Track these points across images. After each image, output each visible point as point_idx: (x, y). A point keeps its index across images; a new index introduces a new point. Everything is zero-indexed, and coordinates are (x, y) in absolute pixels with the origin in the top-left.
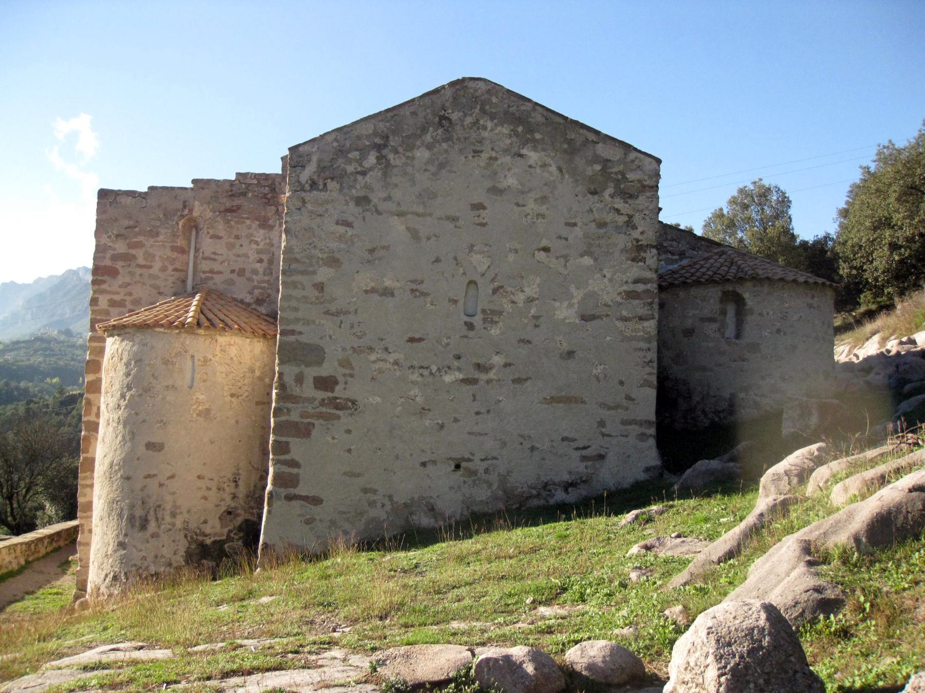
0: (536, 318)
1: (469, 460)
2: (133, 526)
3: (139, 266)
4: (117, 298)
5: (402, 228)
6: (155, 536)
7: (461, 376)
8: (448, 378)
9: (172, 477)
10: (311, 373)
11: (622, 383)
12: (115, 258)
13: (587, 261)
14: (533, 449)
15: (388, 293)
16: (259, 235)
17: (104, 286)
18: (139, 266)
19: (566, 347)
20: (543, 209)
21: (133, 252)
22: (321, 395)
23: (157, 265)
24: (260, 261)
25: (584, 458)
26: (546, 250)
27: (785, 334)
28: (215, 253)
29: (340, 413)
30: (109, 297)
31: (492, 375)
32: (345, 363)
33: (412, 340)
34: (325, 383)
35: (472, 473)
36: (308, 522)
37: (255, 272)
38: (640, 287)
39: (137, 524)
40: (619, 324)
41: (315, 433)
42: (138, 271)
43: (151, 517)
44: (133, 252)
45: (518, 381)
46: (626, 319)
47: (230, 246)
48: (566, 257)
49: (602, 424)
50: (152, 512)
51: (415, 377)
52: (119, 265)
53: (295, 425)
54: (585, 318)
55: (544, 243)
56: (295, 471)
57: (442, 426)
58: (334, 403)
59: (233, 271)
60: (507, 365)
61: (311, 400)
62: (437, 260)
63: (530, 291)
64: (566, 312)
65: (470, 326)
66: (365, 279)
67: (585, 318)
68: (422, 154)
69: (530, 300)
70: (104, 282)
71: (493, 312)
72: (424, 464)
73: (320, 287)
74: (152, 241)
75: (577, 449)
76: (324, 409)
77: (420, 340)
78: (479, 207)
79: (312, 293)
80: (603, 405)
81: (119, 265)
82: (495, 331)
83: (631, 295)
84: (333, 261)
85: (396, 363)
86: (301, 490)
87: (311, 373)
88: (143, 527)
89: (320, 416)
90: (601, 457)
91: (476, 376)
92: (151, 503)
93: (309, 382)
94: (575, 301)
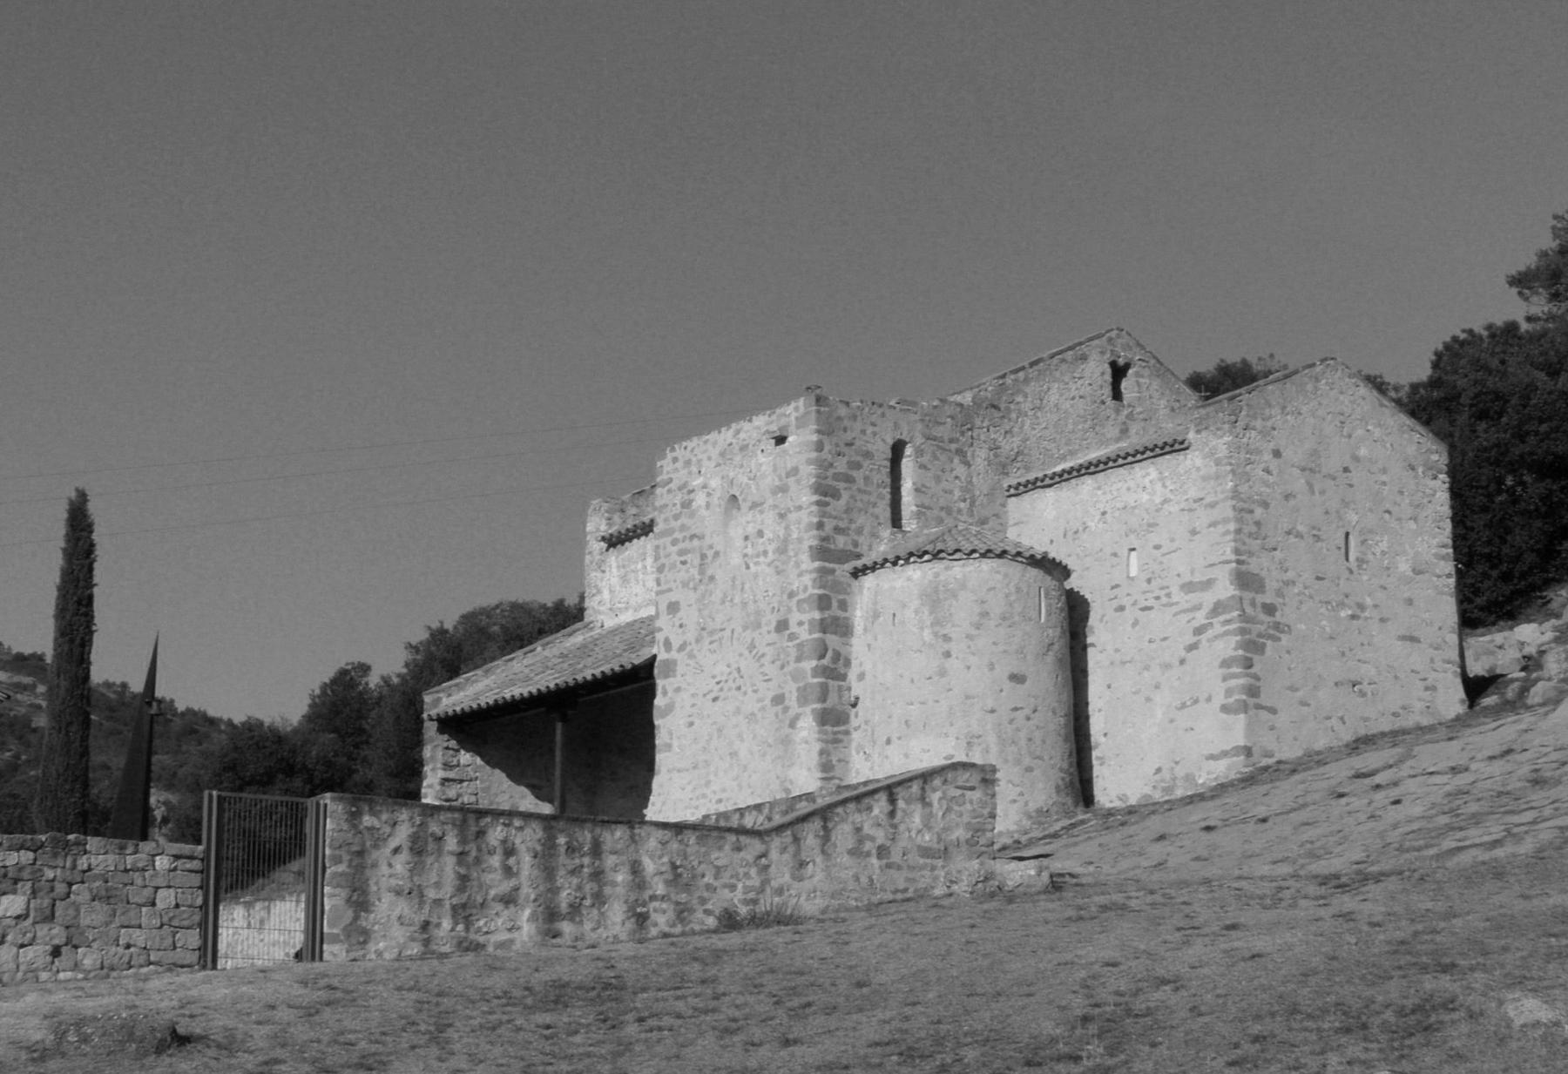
4: (842, 525)
8: (1343, 614)
10: (1260, 599)
12: (836, 477)
14: (1396, 677)
15: (1299, 536)
17: (828, 509)
18: (859, 490)
19: (1406, 595)
20: (1384, 478)
26: (1388, 512)
30: (835, 522)
32: (1279, 593)
33: (1318, 578)
34: (1270, 609)
35: (1362, 694)
37: (960, 511)
38: (1445, 551)
47: (938, 479)
49: (1432, 660)
51: (1323, 610)
52: (841, 485)
53: (1254, 643)
54: (1417, 572)
55: (1388, 506)
58: (1277, 626)
60: (1376, 606)
63: (1384, 546)
64: (1404, 567)
65: (1351, 572)
70: (827, 504)
73: (1258, 524)
78: (1346, 470)
79: (1254, 529)
80: (1431, 646)
82: (1365, 578)
83: (1443, 558)
84: (1265, 505)
87: (1260, 599)
89: (1271, 637)
90: (1433, 688)
93: (1259, 609)
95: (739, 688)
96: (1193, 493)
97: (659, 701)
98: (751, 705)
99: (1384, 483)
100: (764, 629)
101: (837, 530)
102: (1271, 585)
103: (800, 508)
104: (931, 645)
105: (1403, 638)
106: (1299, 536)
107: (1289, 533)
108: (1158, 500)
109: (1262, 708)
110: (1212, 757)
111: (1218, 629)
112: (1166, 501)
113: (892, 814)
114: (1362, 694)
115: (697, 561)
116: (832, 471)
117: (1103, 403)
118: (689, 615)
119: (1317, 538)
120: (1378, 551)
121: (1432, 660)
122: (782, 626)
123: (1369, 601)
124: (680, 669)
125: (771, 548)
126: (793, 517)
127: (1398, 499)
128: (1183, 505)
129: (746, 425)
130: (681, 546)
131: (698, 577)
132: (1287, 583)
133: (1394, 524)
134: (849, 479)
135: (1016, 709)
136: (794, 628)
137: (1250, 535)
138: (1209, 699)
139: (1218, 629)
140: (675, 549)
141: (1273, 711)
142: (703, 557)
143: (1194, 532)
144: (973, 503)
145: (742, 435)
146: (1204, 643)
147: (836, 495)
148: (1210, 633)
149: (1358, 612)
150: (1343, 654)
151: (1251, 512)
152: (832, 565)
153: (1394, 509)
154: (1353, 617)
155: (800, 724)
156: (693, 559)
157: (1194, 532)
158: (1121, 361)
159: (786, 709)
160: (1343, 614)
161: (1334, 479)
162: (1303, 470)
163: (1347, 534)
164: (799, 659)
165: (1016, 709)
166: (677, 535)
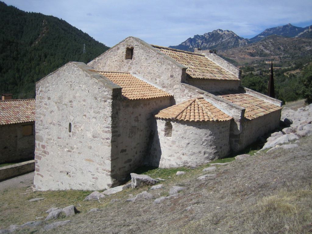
0: (83, 135)
1: (70, 173)
7: (68, 150)
11: (102, 158)
13: (94, 120)
14: (82, 172)
19: (90, 145)
20: (84, 103)
22: (42, 149)
25: (93, 178)
26: (85, 116)
27: (185, 138)
33: (59, 138)
34: (43, 147)
36: (41, 181)
38: (107, 129)
40: (102, 140)
41: (42, 159)
48: (89, 118)
49: (97, 169)
54: (94, 137)
58: (45, 152)
64: (89, 135)
65: (70, 136)
72: (61, 172)
73: (41, 121)
75: (92, 175)
77: (60, 138)
87: (41, 144)
90: (97, 178)
91: (71, 150)
94: (91, 132)
99: (84, 105)
105: (87, 160)
106: (54, 125)
107: (51, 123)
109: (40, 175)
114: (70, 176)
117: (123, 61)
119: (60, 125)
123: (75, 146)
127: (89, 111)
132: (49, 139)
141: (42, 176)
153: (88, 115)
154: (69, 151)
160: (66, 150)
163: (70, 124)
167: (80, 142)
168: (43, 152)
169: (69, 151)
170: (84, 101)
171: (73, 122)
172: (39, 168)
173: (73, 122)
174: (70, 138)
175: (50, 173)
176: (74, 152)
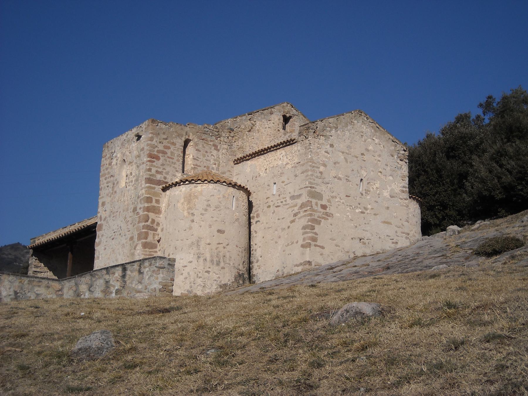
0: (379, 194)
2: (213, 264)
3: (168, 157)
4: (160, 170)
5: (343, 157)
6: (223, 268)
8: (357, 211)
9: (228, 245)
10: (320, 203)
12: (158, 151)
13: (391, 178)
14: (380, 238)
15: (340, 179)
16: (215, 152)
17: (154, 164)
18: (168, 157)
19: (386, 205)
20: (379, 159)
21: (166, 150)
22: (323, 211)
23: (176, 158)
24: (215, 164)
25: (393, 243)
26: (381, 172)
28: (198, 157)
29: (329, 218)
30: (157, 169)
31: (368, 211)
32: (329, 201)
34: (324, 207)
35: (364, 244)
36: (321, 255)
37: (213, 168)
38: (404, 189)
39: (215, 263)
40: (400, 200)
41: (322, 224)
42: (168, 160)
43: (221, 260)
44: (166, 150)
45: (375, 214)
46: (401, 199)
48: (386, 175)
49: (396, 232)
50: (222, 258)
51: (348, 209)
52: (160, 155)
53: (316, 220)
54: (392, 197)
55: (380, 170)
56: (316, 236)
57: (356, 227)
58: (327, 214)
59: (205, 167)
60: (372, 209)
61: (320, 212)
62: (353, 170)
63: (377, 185)
64: (386, 194)
66: (333, 173)
67: (392, 197)
68: (347, 133)
69: (377, 188)
70: (154, 162)
71: (368, 191)
72: (352, 239)
73: (321, 173)
74: (173, 147)
76: (324, 216)
77: (349, 196)
78: (362, 154)
79: (319, 175)
80: (396, 226)
81: (160, 155)
82: (368, 197)
83: (403, 192)
84: (325, 165)
85: (343, 203)
86: (318, 243)
87: (320, 203)
88: (218, 264)
89: (323, 218)
90: (397, 243)
92: (221, 254)
93: (319, 206)
95: (120, 234)
96: (296, 161)
97: (97, 240)
98: (124, 241)
99: (379, 161)
100: (129, 211)
101: (157, 172)
102: (326, 197)
103: (143, 163)
104: (187, 217)
105: (384, 222)
107: (335, 177)
108: (285, 163)
110: (297, 265)
111: (302, 214)
112: (287, 164)
113: (124, 276)
114: (364, 244)
115: (112, 186)
116: (156, 149)
117: (279, 131)
118: (108, 207)
120: (375, 187)
121: (396, 232)
122: (135, 209)
123: (369, 207)
124: (104, 227)
125: (134, 179)
126: (141, 167)
128: (292, 165)
129: (130, 132)
130: (108, 180)
131: (111, 192)
132: (333, 197)
133: (383, 177)
134: (164, 153)
135: (219, 244)
136: (138, 210)
137: (317, 177)
138: (297, 242)
139: (302, 214)
140: (106, 181)
141: (323, 248)
142: (114, 184)
143: (296, 176)
144: (219, 165)
145: (129, 136)
146: (297, 220)
147: (158, 158)
148: (299, 216)
149: (364, 211)
150: (356, 227)
151: (319, 168)
152: (154, 186)
154: (362, 212)
155: (137, 248)
156: (111, 185)
157: (296, 176)
158: (288, 115)
159: (134, 242)
160: (357, 211)
161: (357, 157)
162: (343, 153)
164: (139, 222)
165: (219, 244)
166: (107, 176)
167: (375, 201)
168: (323, 214)
169: (362, 212)
170: (379, 156)
171: (366, 178)
172: (316, 236)
173: (366, 178)
174: (362, 197)
175: (334, 242)
176: (368, 213)
